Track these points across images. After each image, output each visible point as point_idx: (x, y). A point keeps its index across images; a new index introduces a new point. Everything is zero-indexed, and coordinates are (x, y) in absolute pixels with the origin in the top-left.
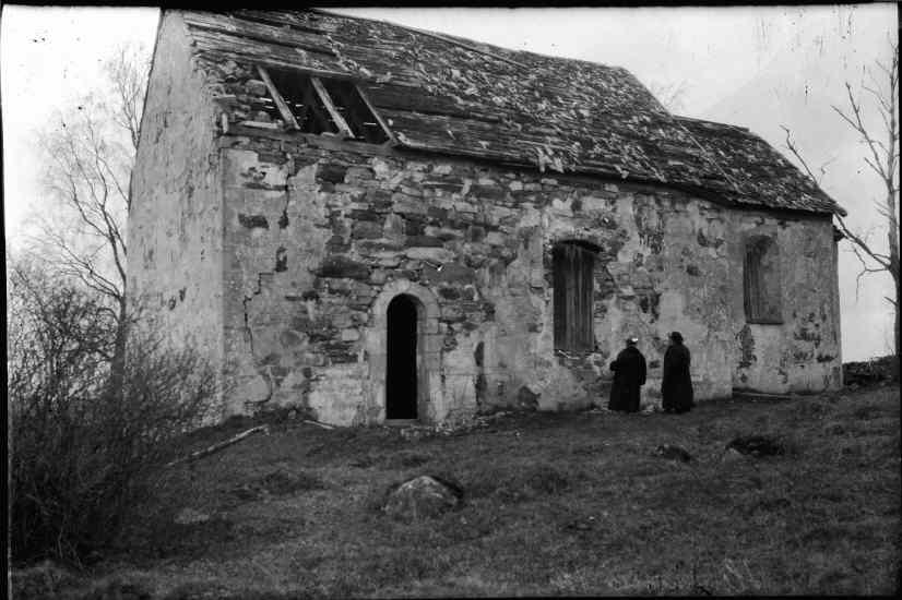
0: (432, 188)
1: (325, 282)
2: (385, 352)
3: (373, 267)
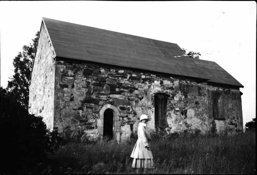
1: (85, 104)
2: (103, 126)
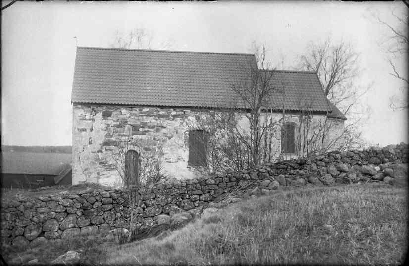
0: (142, 116)
1: (104, 147)
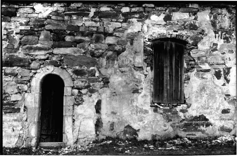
3: (32, 60)
